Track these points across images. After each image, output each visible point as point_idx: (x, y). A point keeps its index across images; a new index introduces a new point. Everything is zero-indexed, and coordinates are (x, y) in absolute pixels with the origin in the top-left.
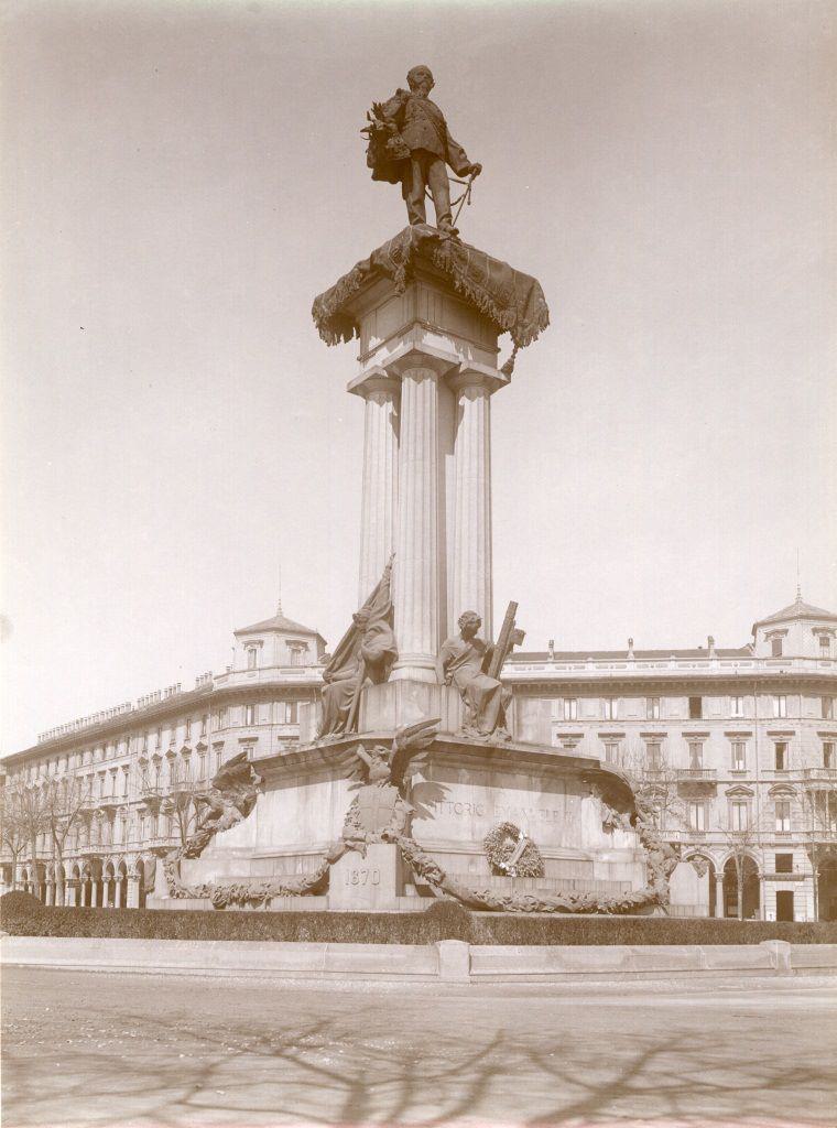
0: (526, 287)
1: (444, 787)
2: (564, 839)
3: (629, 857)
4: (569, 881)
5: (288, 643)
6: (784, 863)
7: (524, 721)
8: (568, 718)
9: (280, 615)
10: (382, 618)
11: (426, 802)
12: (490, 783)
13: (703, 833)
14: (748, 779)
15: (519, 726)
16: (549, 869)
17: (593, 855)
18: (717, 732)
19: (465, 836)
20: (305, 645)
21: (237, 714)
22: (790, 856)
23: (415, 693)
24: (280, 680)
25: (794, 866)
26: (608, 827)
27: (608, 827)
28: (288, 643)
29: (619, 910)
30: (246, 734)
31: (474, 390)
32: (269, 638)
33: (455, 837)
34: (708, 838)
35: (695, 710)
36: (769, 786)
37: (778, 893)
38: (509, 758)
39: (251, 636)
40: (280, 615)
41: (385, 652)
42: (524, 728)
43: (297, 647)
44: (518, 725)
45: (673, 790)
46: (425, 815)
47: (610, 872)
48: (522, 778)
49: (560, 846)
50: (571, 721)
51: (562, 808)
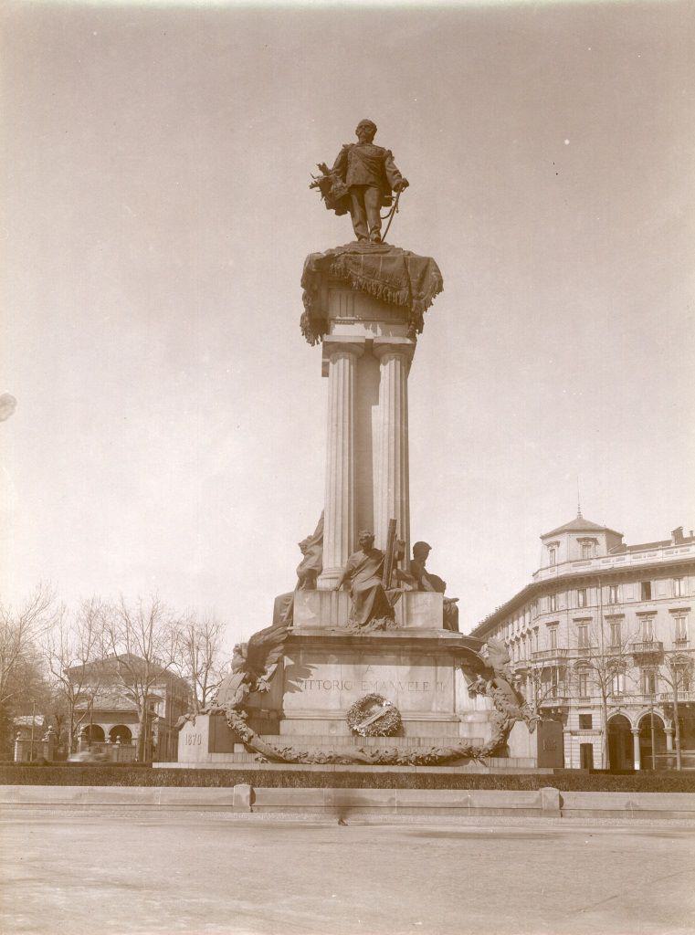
0: (420, 268)
1: (311, 667)
2: (434, 704)
3: (483, 717)
4: (414, 738)
5: (579, 540)
6: (586, 722)
7: (413, 611)
8: (677, 594)
9: (580, 518)
10: (316, 544)
11: (297, 681)
12: (360, 662)
13: (622, 697)
14: (687, 648)
15: (409, 617)
16: (411, 730)
17: (461, 717)
18: (663, 609)
19: (334, 705)
20: (595, 540)
21: (544, 602)
22: (590, 716)
23: (307, 600)
24: (602, 568)
25: (593, 724)
26: (473, 694)
27: (473, 694)
28: (579, 540)
29: (420, 761)
30: (551, 619)
31: (387, 357)
32: (563, 539)
33: (322, 706)
34: (626, 701)
35: (647, 593)
36: (575, 661)
37: (582, 745)
38: (369, 643)
39: (551, 539)
40: (580, 518)
41: (310, 570)
42: (414, 617)
43: (586, 542)
44: (408, 614)
45: (630, 660)
46: (293, 689)
47: (470, 731)
48: (392, 657)
49: (430, 711)
50: (680, 597)
51: (433, 678)
